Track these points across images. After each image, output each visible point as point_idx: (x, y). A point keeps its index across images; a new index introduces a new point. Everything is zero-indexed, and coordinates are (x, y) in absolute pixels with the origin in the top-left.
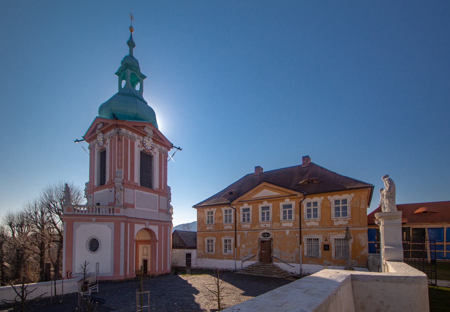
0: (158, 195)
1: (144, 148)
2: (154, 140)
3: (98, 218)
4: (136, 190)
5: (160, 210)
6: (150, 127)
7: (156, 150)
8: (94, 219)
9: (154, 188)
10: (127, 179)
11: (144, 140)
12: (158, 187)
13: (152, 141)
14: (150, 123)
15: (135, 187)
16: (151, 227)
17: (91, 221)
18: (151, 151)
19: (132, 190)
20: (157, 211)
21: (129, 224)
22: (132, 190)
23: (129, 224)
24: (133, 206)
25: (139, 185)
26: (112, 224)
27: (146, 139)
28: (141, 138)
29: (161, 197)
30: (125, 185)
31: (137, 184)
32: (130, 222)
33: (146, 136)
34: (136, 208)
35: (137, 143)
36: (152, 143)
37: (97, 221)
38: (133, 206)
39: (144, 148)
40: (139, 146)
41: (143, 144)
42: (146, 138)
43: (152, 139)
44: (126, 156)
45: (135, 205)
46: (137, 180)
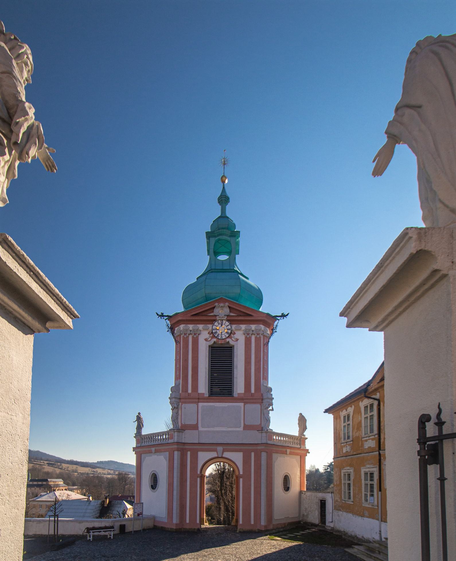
0: (242, 404)
1: (215, 340)
2: (231, 321)
3: (157, 448)
4: (201, 404)
5: (247, 427)
6: (222, 305)
8: (153, 449)
9: (235, 395)
10: (187, 391)
12: (243, 392)
13: (227, 323)
14: (221, 298)
15: (200, 399)
16: (226, 455)
17: (150, 452)
18: (228, 340)
19: (195, 405)
20: (241, 429)
21: (189, 453)
22: (193, 406)
23: (189, 453)
24: (195, 427)
25: (207, 395)
26: (167, 453)
27: (217, 326)
29: (248, 406)
30: (182, 400)
31: (203, 394)
32: (190, 450)
33: (215, 320)
34: (201, 429)
35: (204, 335)
36: (229, 327)
37: (156, 451)
38: (195, 427)
39: (215, 340)
40: (206, 340)
41: (213, 334)
42: (216, 324)
46: (203, 388)
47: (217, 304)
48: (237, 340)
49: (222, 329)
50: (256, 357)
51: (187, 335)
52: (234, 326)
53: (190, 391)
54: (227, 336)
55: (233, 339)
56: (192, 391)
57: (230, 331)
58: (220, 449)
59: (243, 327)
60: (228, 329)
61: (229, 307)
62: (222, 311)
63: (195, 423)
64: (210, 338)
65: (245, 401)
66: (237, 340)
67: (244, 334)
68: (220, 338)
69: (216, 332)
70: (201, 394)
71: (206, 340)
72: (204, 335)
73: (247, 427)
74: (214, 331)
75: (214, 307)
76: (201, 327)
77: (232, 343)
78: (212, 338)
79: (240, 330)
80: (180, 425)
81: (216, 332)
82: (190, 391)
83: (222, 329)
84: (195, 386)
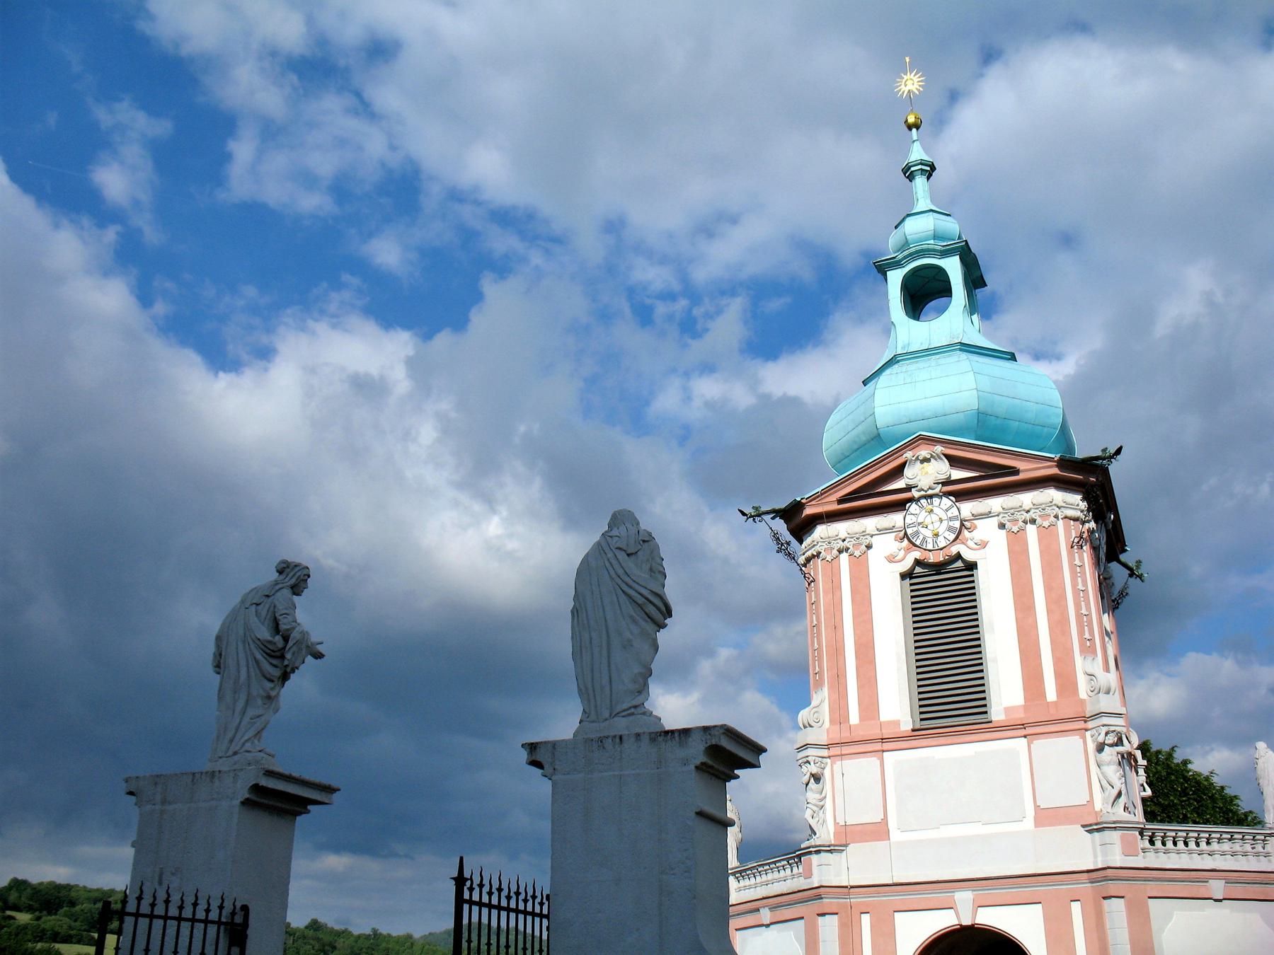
6: (924, 452)
7: (986, 530)
9: (997, 713)
11: (909, 519)
13: (946, 502)
15: (888, 741)
18: (954, 550)
19: (873, 761)
20: (1029, 823)
23: (866, 919)
24: (879, 831)
28: (896, 519)
29: (1039, 744)
31: (897, 723)
33: (911, 500)
34: (895, 835)
36: (954, 512)
39: (917, 554)
40: (891, 559)
42: (913, 508)
43: (948, 494)
44: (837, 628)
45: (892, 824)
47: (909, 455)
48: (983, 545)
49: (934, 523)
50: (1048, 589)
51: (835, 552)
52: (968, 508)
53: (854, 718)
54: (952, 537)
55: (970, 543)
56: (861, 719)
57: (957, 524)
58: (964, 897)
59: (995, 503)
60: (950, 519)
61: (947, 456)
62: (926, 472)
63: (878, 818)
64: (902, 553)
65: (1029, 731)
66: (983, 545)
67: (1002, 526)
68: (930, 547)
69: (917, 533)
70: (889, 723)
71: (891, 559)
72: (886, 545)
73: (1046, 817)
74: (909, 531)
75: (903, 465)
76: (870, 523)
77: (969, 555)
78: (908, 550)
79: (988, 515)
80: (832, 829)
81: (917, 533)
82: (854, 718)
83: (934, 523)
84: (870, 704)
